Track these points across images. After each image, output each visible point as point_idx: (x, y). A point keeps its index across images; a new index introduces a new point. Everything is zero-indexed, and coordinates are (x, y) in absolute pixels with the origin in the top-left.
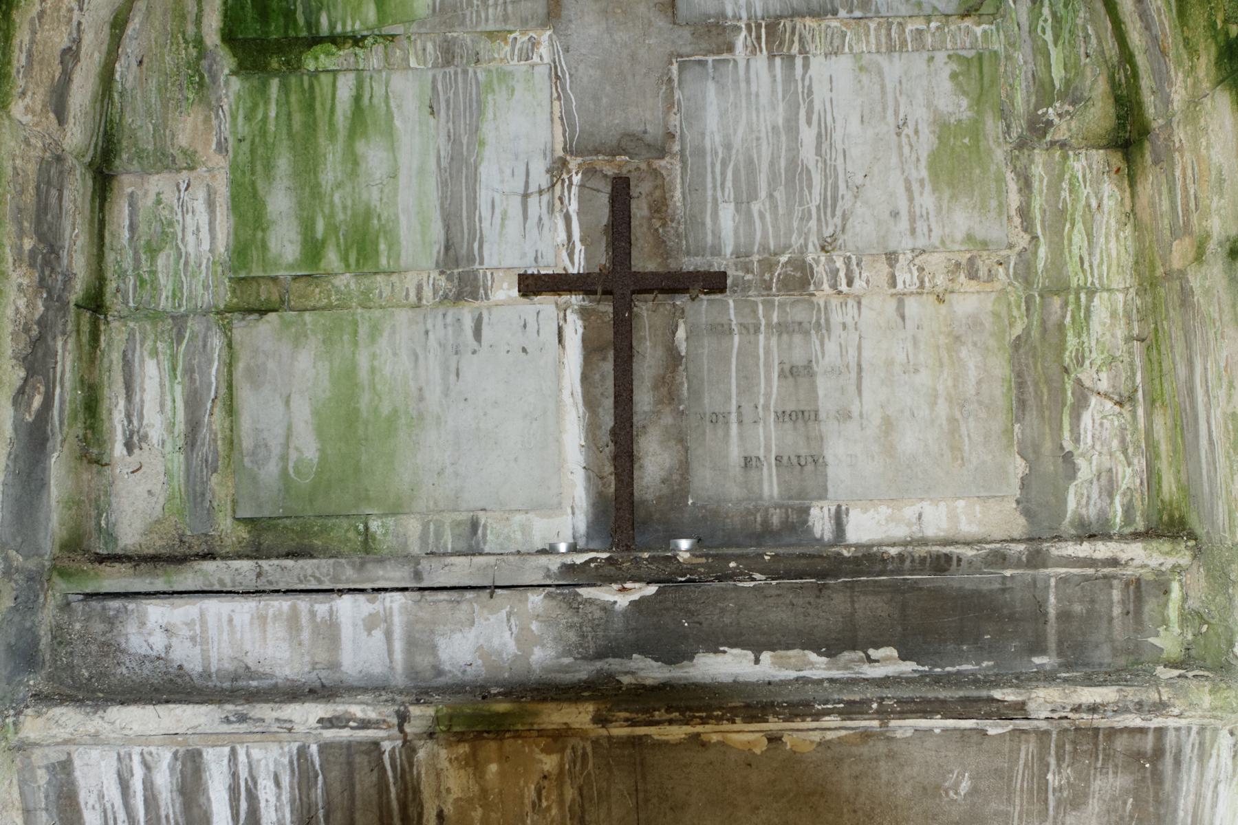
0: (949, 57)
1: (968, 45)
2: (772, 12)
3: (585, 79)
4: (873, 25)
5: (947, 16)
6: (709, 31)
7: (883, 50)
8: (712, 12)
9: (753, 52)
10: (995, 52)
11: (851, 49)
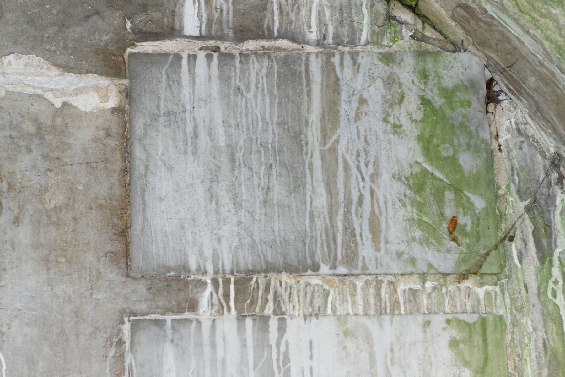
0: (448, 321)
1: (469, 308)
2: (242, 266)
3: (19, 339)
4: (359, 284)
5: (445, 275)
6: (169, 286)
7: (372, 312)
8: (172, 264)
9: (221, 311)
10: (501, 318)
11: (334, 311)
